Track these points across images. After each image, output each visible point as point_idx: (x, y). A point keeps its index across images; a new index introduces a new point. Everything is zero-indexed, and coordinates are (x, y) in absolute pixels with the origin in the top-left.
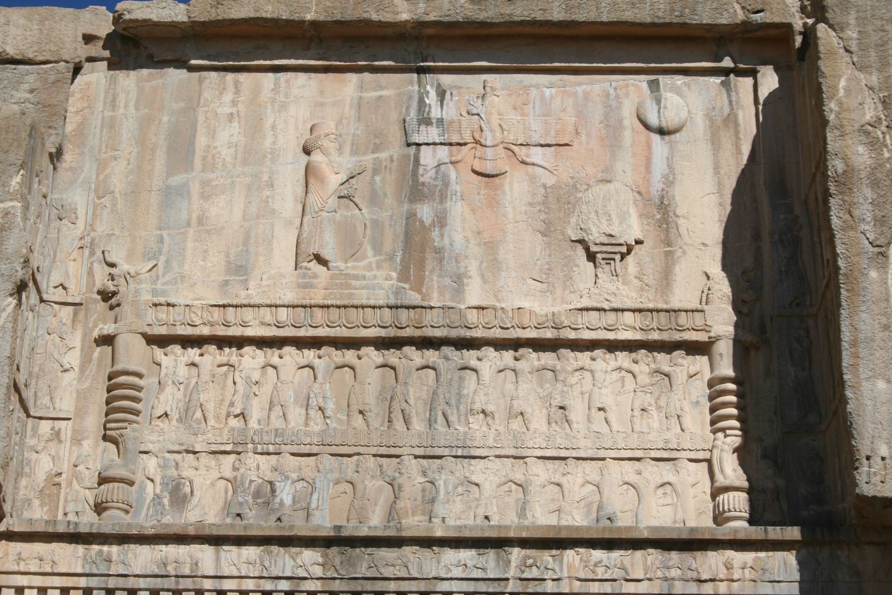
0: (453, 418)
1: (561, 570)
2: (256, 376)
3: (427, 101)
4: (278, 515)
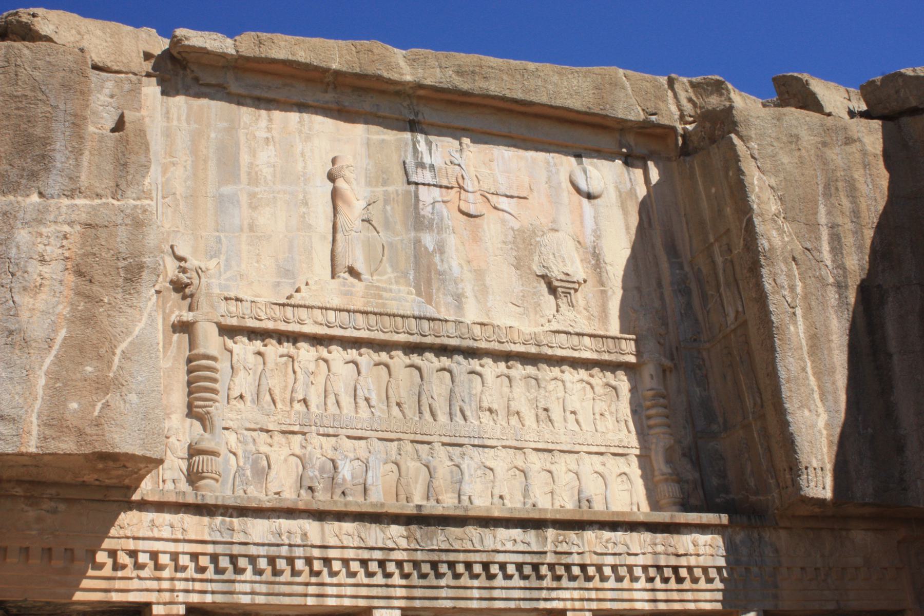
0: (468, 413)
1: (583, 545)
2: (312, 367)
3: (420, 149)
4: (342, 489)
